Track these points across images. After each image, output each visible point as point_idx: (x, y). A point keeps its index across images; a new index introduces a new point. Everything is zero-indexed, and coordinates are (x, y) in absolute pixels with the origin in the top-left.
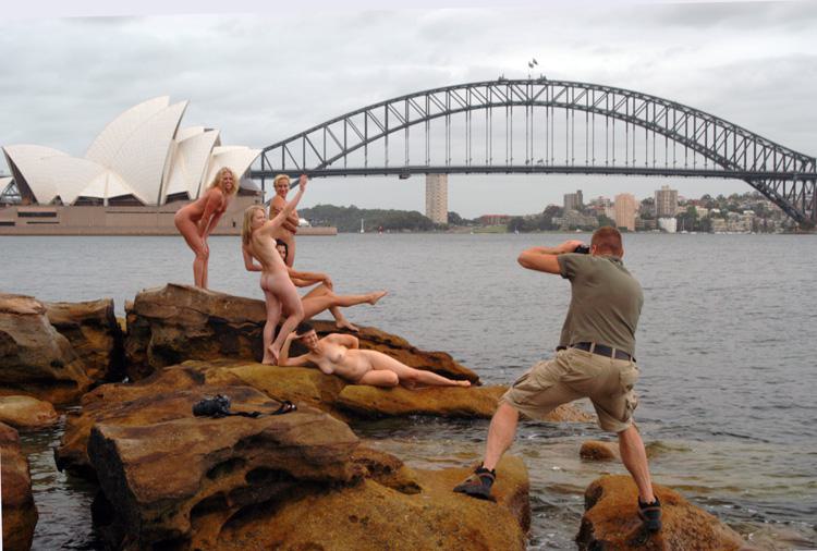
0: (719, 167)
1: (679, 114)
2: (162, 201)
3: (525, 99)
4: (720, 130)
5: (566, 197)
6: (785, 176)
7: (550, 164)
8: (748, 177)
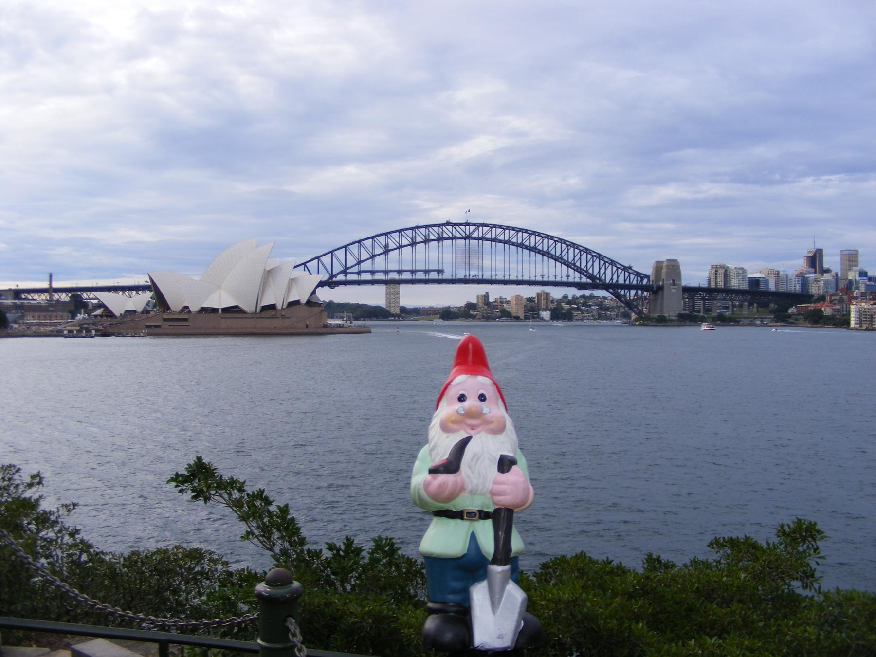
0: (589, 281)
2: (258, 311)
3: (464, 235)
4: (589, 256)
6: (630, 287)
7: (480, 277)
8: (606, 287)
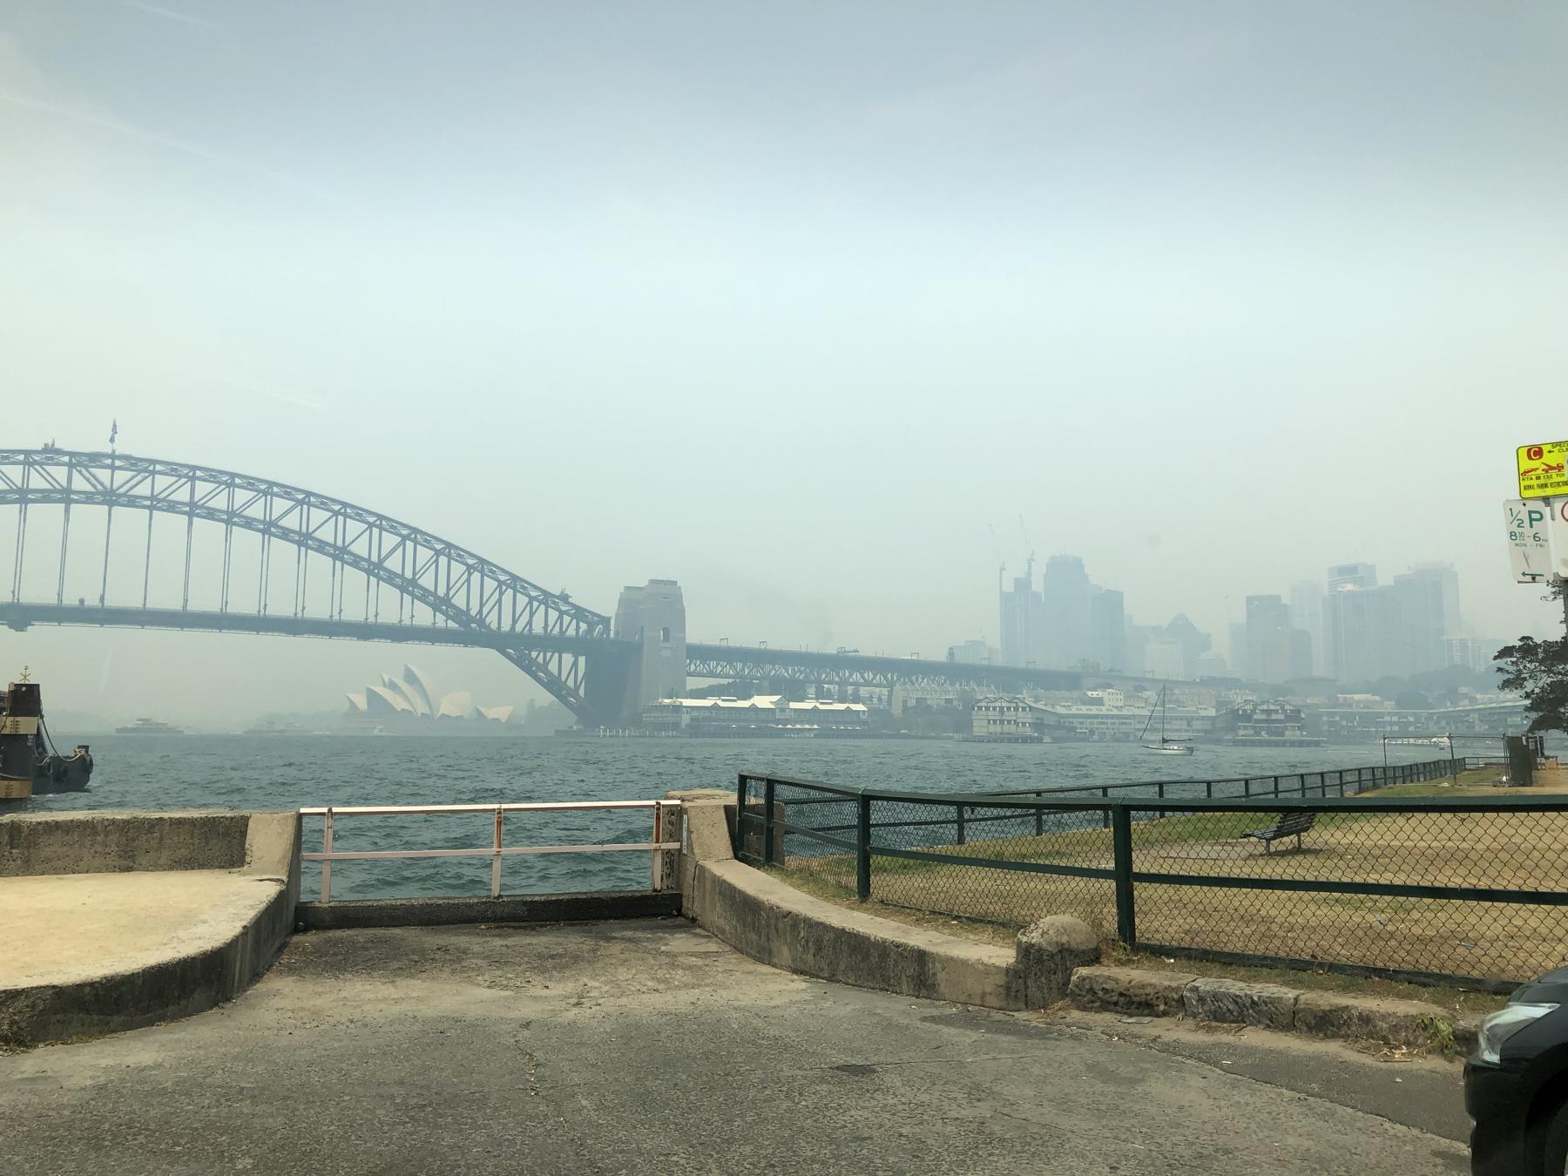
0: (452, 624)
1: (458, 569)
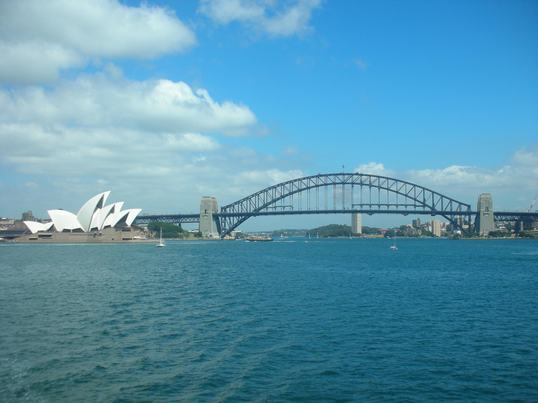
5: (413, 221)
